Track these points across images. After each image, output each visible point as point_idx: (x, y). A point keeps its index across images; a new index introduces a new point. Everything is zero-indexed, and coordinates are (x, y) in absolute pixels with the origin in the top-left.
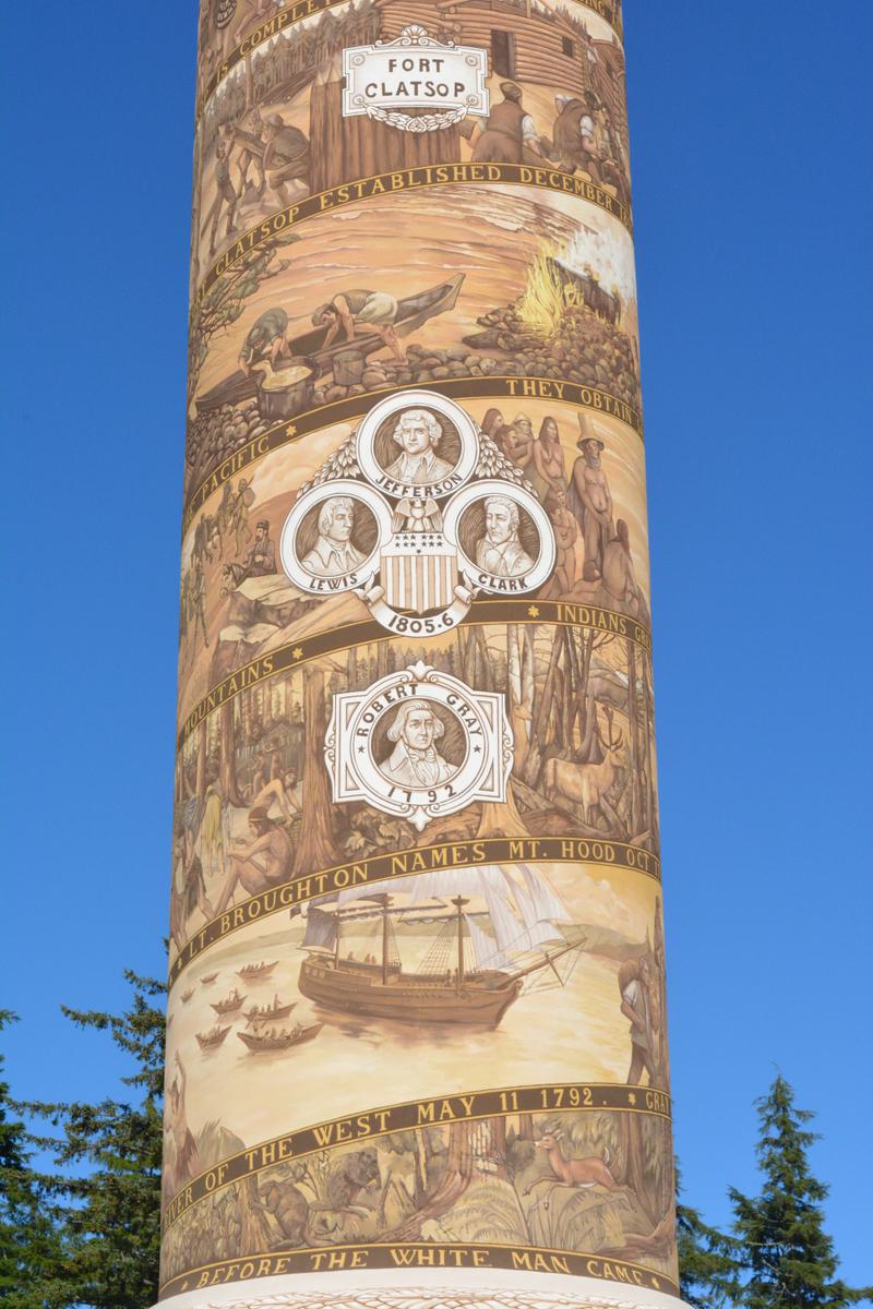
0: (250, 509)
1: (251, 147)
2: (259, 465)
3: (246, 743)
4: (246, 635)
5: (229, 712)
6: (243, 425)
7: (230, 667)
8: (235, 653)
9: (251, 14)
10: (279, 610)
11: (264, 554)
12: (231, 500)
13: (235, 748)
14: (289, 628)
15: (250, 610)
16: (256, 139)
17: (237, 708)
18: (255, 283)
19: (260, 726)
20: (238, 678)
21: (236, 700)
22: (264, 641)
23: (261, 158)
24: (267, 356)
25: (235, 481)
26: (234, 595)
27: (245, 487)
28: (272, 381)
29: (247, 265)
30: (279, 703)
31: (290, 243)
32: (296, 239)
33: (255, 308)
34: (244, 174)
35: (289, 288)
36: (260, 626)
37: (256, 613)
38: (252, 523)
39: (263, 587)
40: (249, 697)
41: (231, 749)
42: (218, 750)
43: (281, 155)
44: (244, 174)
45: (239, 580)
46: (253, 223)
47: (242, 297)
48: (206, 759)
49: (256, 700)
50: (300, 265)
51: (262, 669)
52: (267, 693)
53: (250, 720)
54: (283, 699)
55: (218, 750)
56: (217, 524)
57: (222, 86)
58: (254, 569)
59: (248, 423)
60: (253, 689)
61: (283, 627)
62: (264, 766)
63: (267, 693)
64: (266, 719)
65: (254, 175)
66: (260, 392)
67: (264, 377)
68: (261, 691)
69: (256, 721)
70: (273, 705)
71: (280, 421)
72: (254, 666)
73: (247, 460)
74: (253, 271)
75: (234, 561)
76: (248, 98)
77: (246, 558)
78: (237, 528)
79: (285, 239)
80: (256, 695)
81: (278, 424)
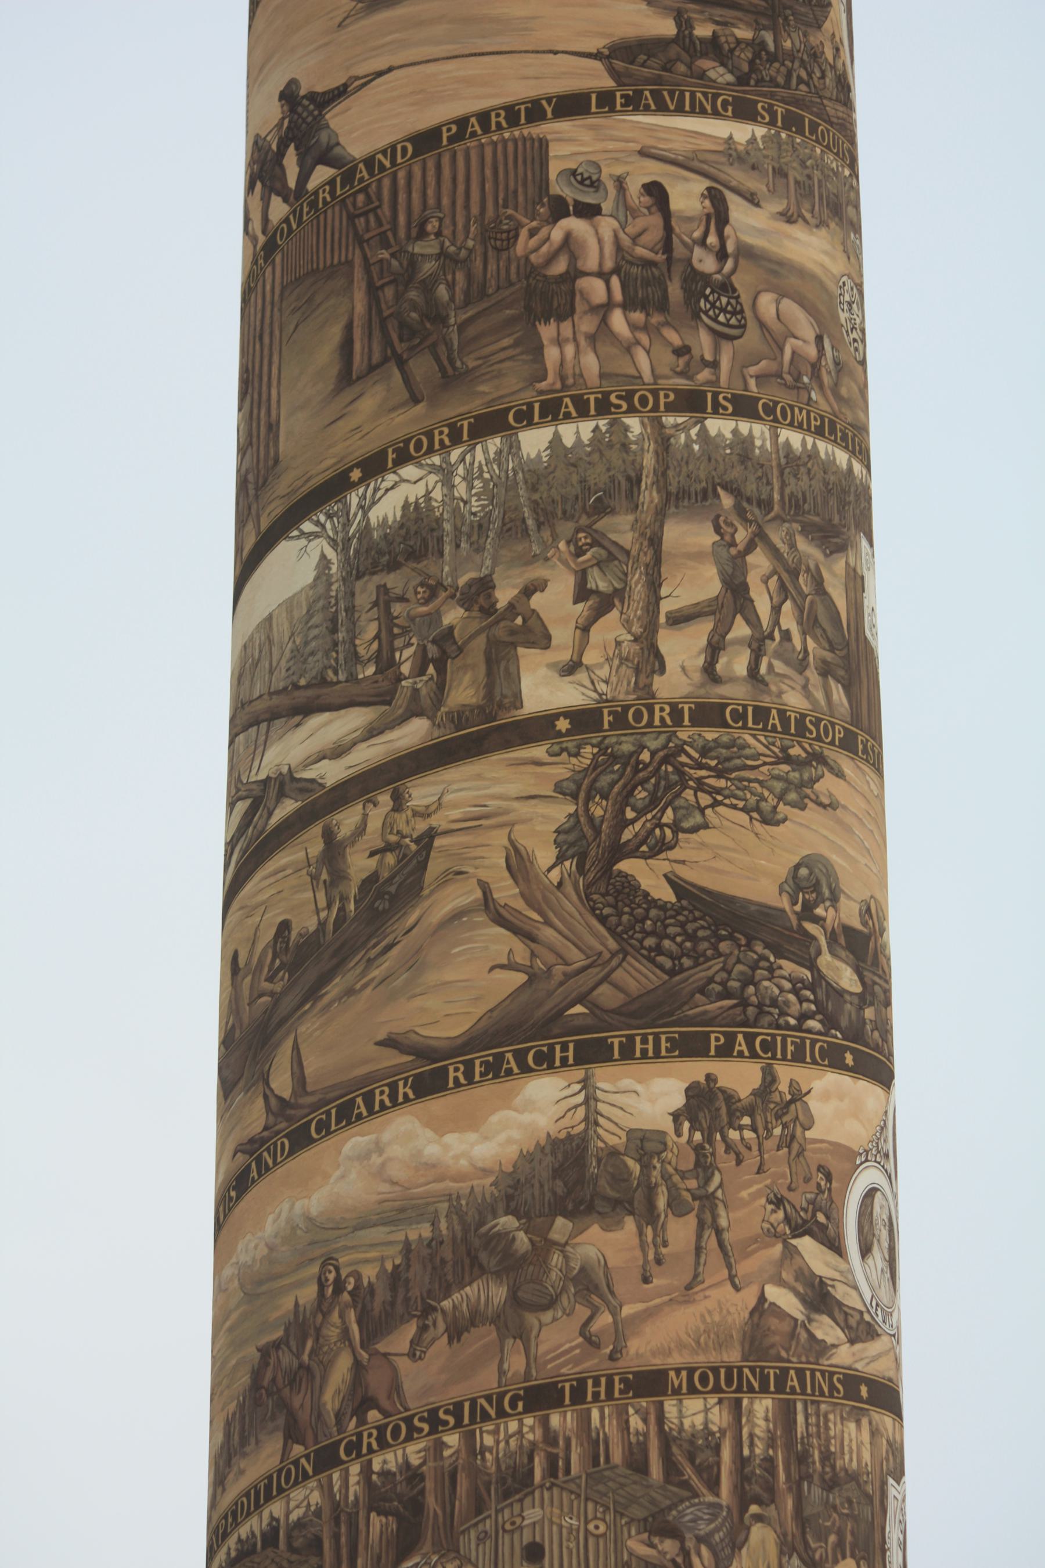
0: (809, 1134)
1: (785, 576)
2: (820, 1078)
3: (816, 1478)
4: (810, 1320)
5: (786, 1414)
6: (791, 997)
7: (787, 1351)
8: (793, 1335)
9: (773, 367)
10: (846, 1314)
11: (828, 1217)
12: (776, 1097)
13: (801, 1479)
14: (858, 1346)
15: (812, 1286)
16: (794, 574)
17: (800, 1418)
18: (802, 793)
19: (833, 1467)
20: (800, 1373)
21: (799, 1406)
22: (834, 1346)
23: (802, 611)
24: (818, 920)
25: (786, 1073)
26: (791, 1253)
27: (798, 1095)
28: (828, 964)
29: (788, 759)
30: (851, 1452)
31: (837, 775)
32: (840, 774)
33: (803, 834)
34: (776, 610)
35: (832, 837)
36: (825, 1319)
37: (819, 1297)
38: (813, 1158)
39: (827, 1264)
40: (818, 1416)
41: (795, 1476)
42: (769, 1463)
43: (824, 630)
44: (776, 610)
45: (800, 1229)
46: (794, 701)
47: (781, 798)
48: (741, 1462)
49: (827, 1428)
50: (849, 819)
51: (832, 1388)
52: (839, 1426)
53: (821, 1452)
54: (854, 1447)
55: (769, 1463)
56: (750, 1111)
57: (720, 426)
58: (815, 1229)
59: (801, 1003)
60: (823, 1407)
61: (852, 1342)
62: (839, 1528)
63: (839, 1426)
64: (839, 1463)
65: (788, 621)
66: (812, 966)
67: (819, 953)
68: (831, 1417)
69: (827, 1457)
70: (846, 1449)
71: (839, 1035)
72: (823, 1372)
73: (799, 1057)
74: (797, 775)
75: (785, 1193)
76: (776, 496)
77: (804, 1204)
78: (789, 1147)
79: (832, 763)
80: (827, 1421)
81: (836, 1037)
